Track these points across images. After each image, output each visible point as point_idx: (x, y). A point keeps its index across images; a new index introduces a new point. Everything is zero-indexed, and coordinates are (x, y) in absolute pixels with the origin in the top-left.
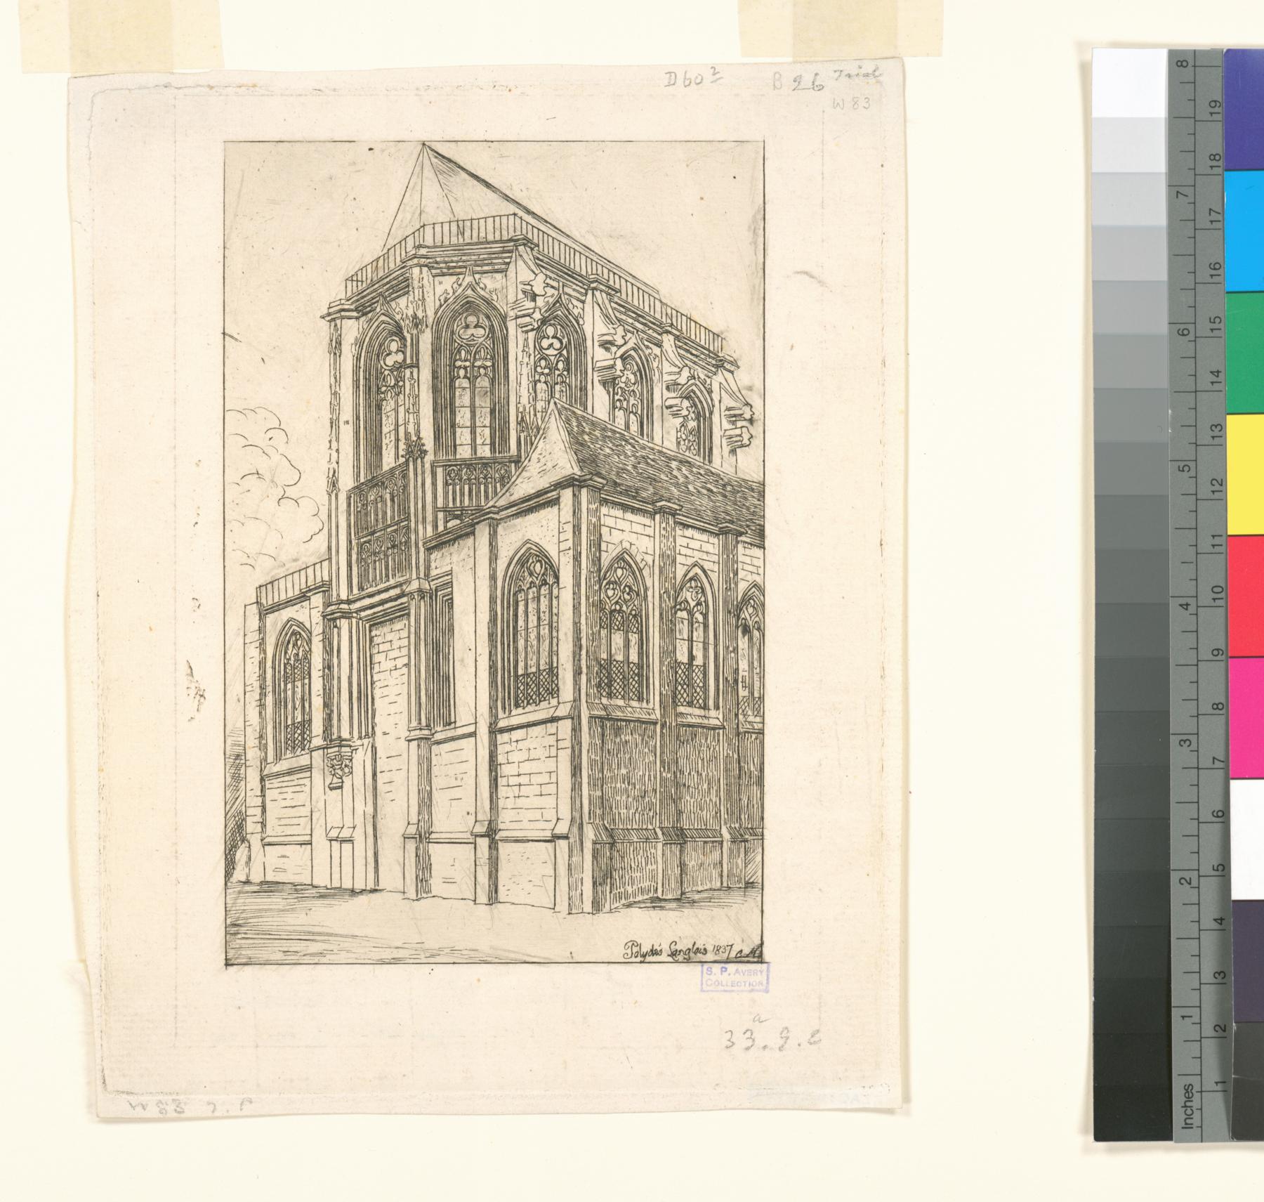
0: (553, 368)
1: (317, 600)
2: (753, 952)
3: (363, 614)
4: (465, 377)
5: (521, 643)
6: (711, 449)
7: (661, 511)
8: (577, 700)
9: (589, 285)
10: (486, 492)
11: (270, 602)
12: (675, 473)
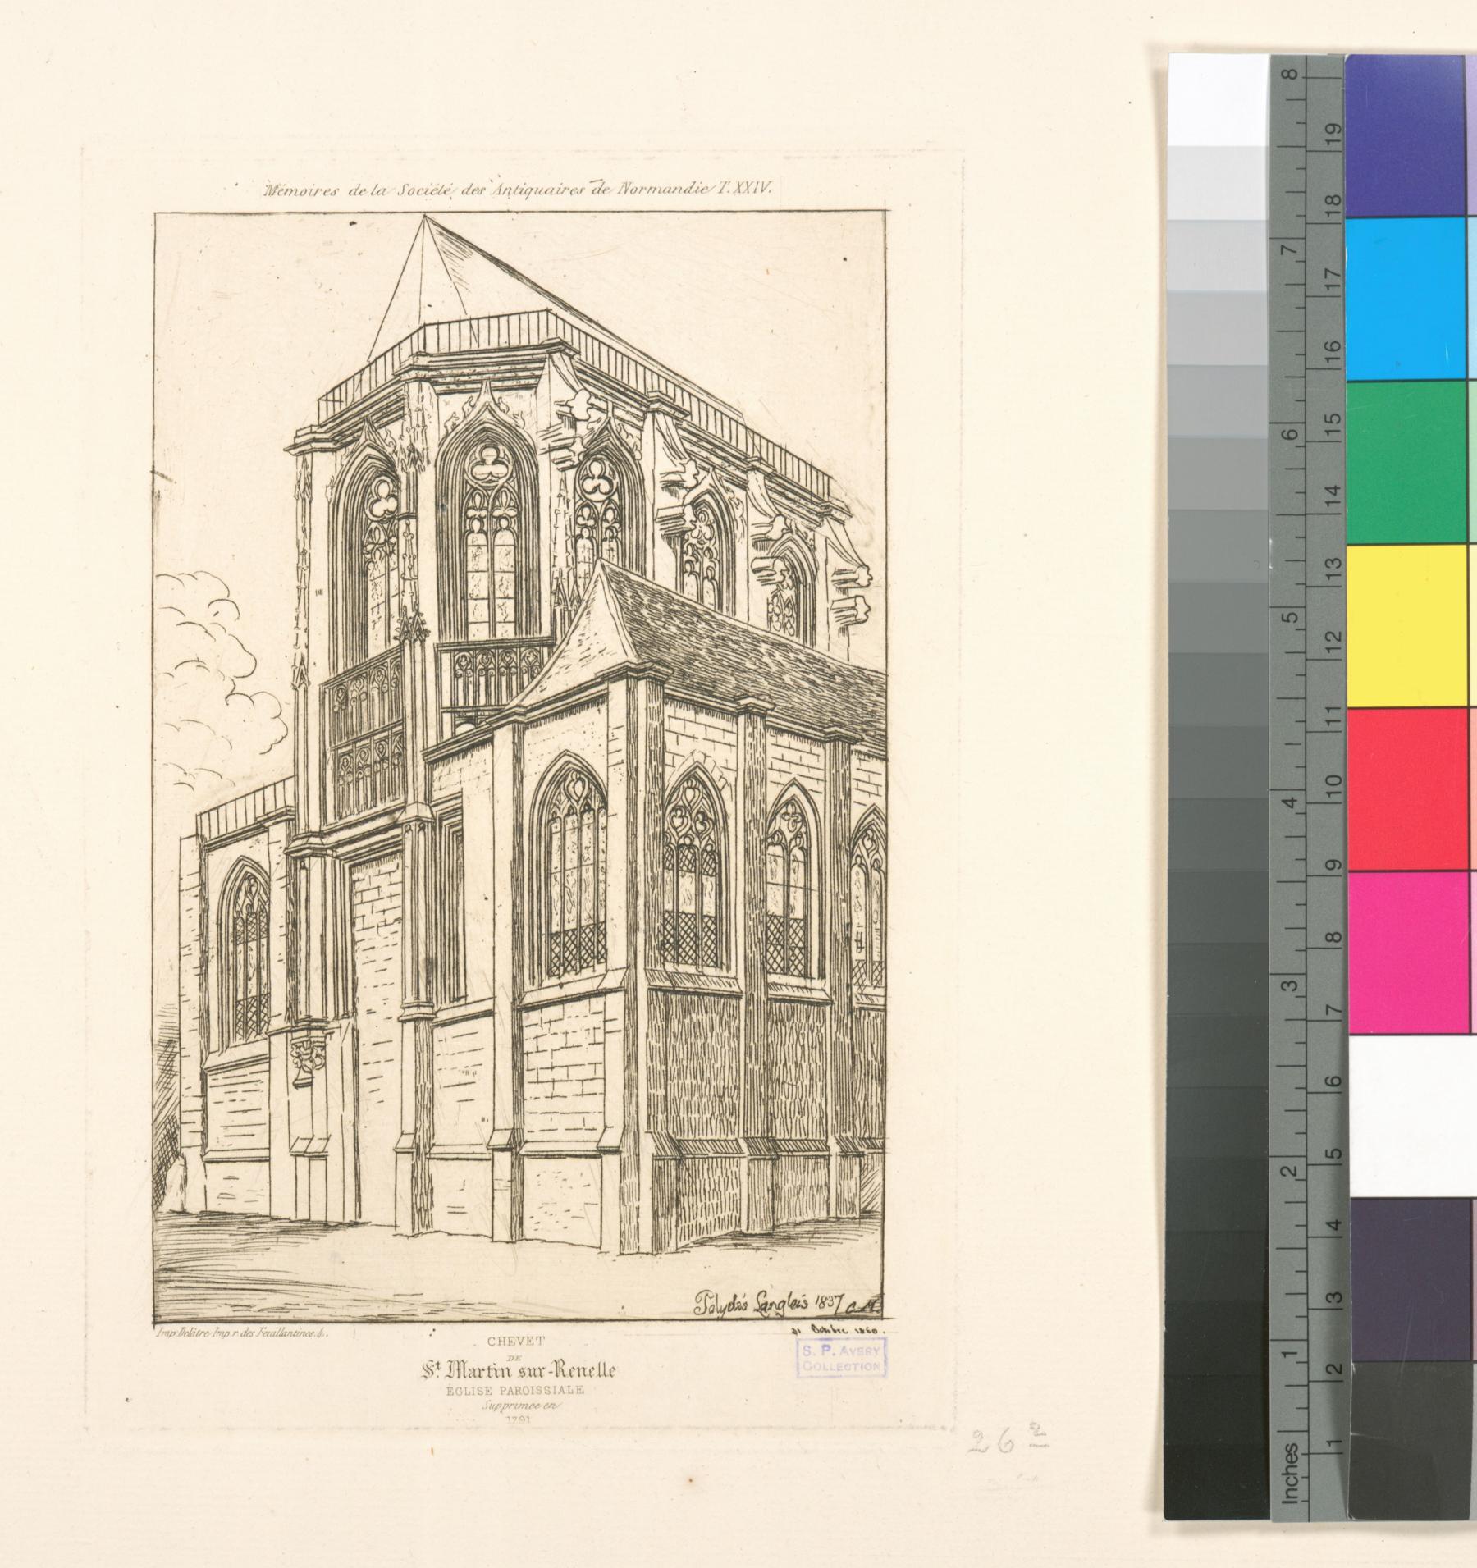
0: (598, 519)
1: (278, 832)
2: (871, 1304)
3: (340, 851)
4: (481, 531)
5: (556, 890)
6: (814, 627)
7: (746, 711)
8: (631, 967)
9: (648, 405)
10: (509, 688)
11: (214, 834)
12: (766, 659)
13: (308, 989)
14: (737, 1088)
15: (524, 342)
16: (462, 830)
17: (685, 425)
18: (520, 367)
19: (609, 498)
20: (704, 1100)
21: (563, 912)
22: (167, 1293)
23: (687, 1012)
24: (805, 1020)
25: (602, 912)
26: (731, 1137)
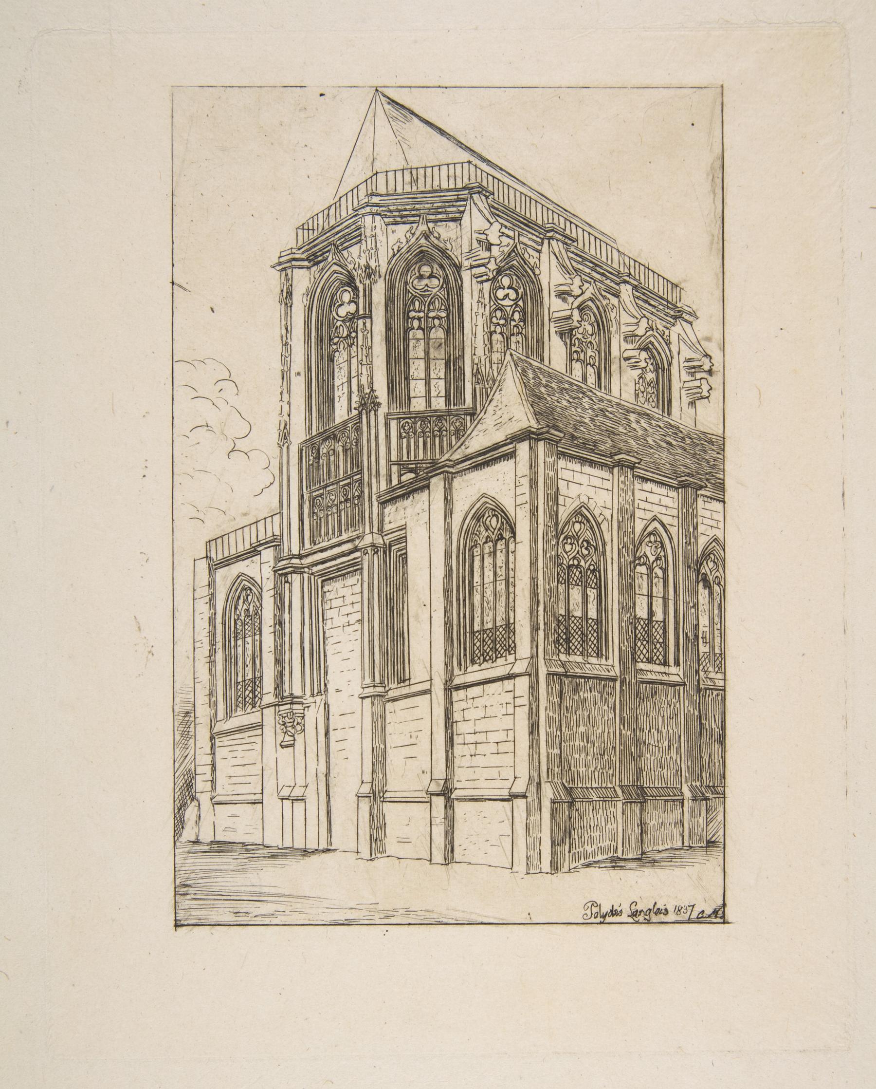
0: (508, 319)
1: (268, 555)
2: (715, 912)
3: (315, 569)
4: (420, 328)
5: (477, 598)
6: (670, 401)
7: (620, 464)
8: (534, 657)
9: (546, 233)
10: (441, 447)
11: (220, 557)
12: (634, 425)
13: (291, 673)
14: (614, 748)
15: (452, 186)
16: (406, 553)
17: (572, 249)
18: (450, 205)
19: (517, 305)
20: (589, 758)
21: (482, 613)
22: (185, 903)
23: (575, 690)
24: (665, 698)
25: (511, 614)
26: (609, 785)
